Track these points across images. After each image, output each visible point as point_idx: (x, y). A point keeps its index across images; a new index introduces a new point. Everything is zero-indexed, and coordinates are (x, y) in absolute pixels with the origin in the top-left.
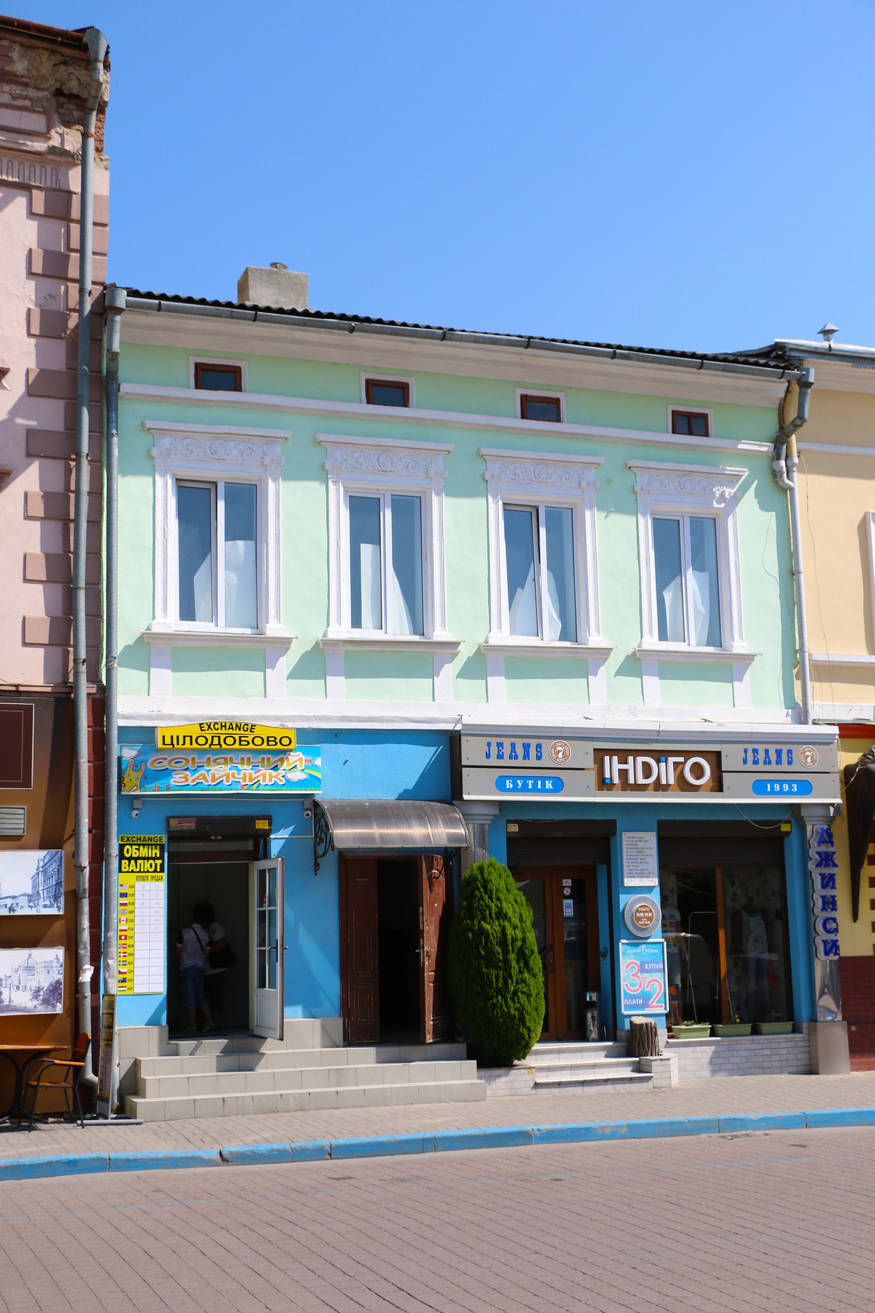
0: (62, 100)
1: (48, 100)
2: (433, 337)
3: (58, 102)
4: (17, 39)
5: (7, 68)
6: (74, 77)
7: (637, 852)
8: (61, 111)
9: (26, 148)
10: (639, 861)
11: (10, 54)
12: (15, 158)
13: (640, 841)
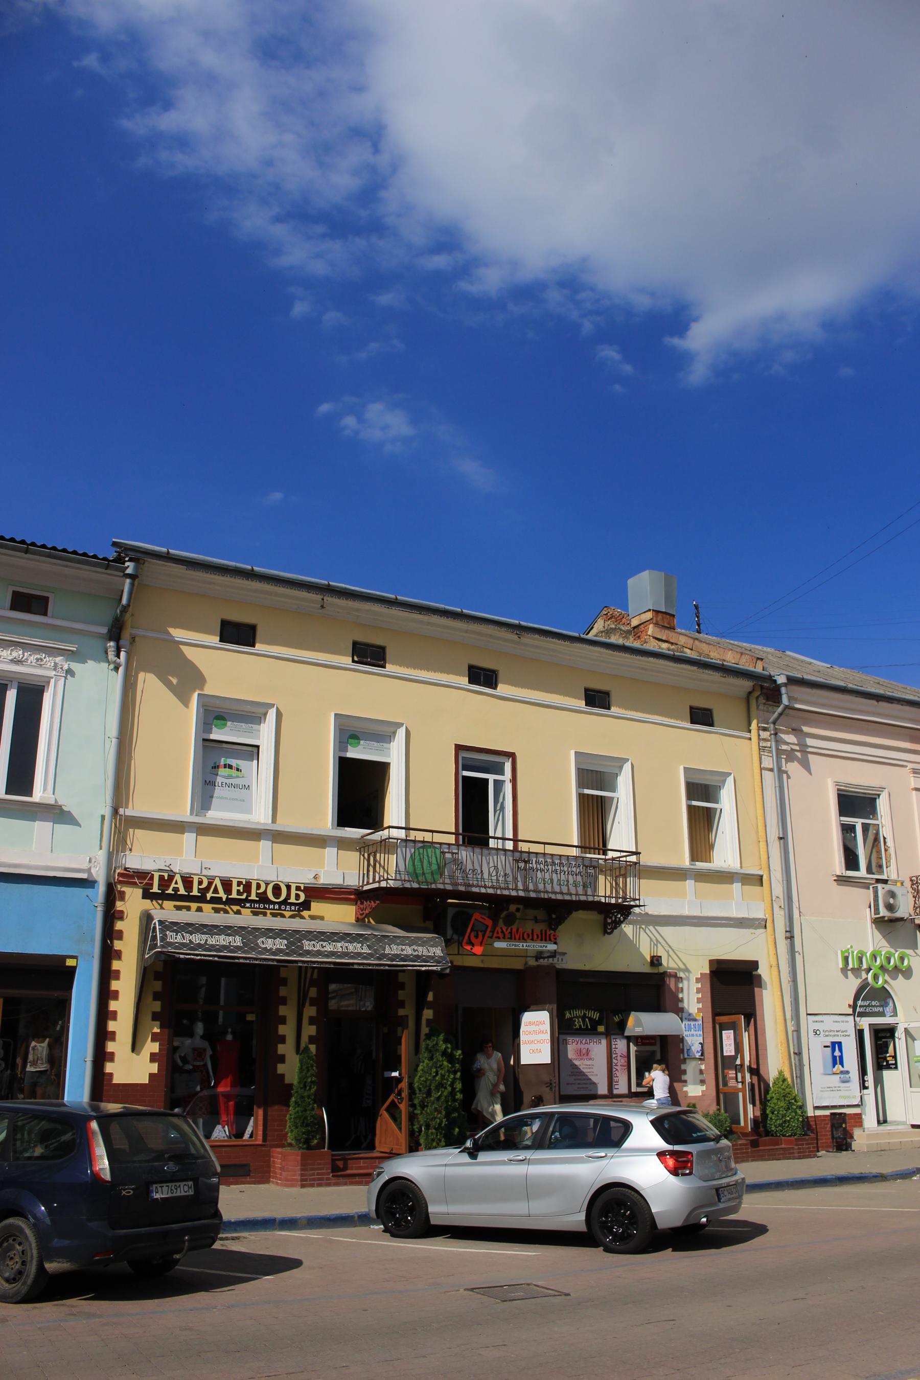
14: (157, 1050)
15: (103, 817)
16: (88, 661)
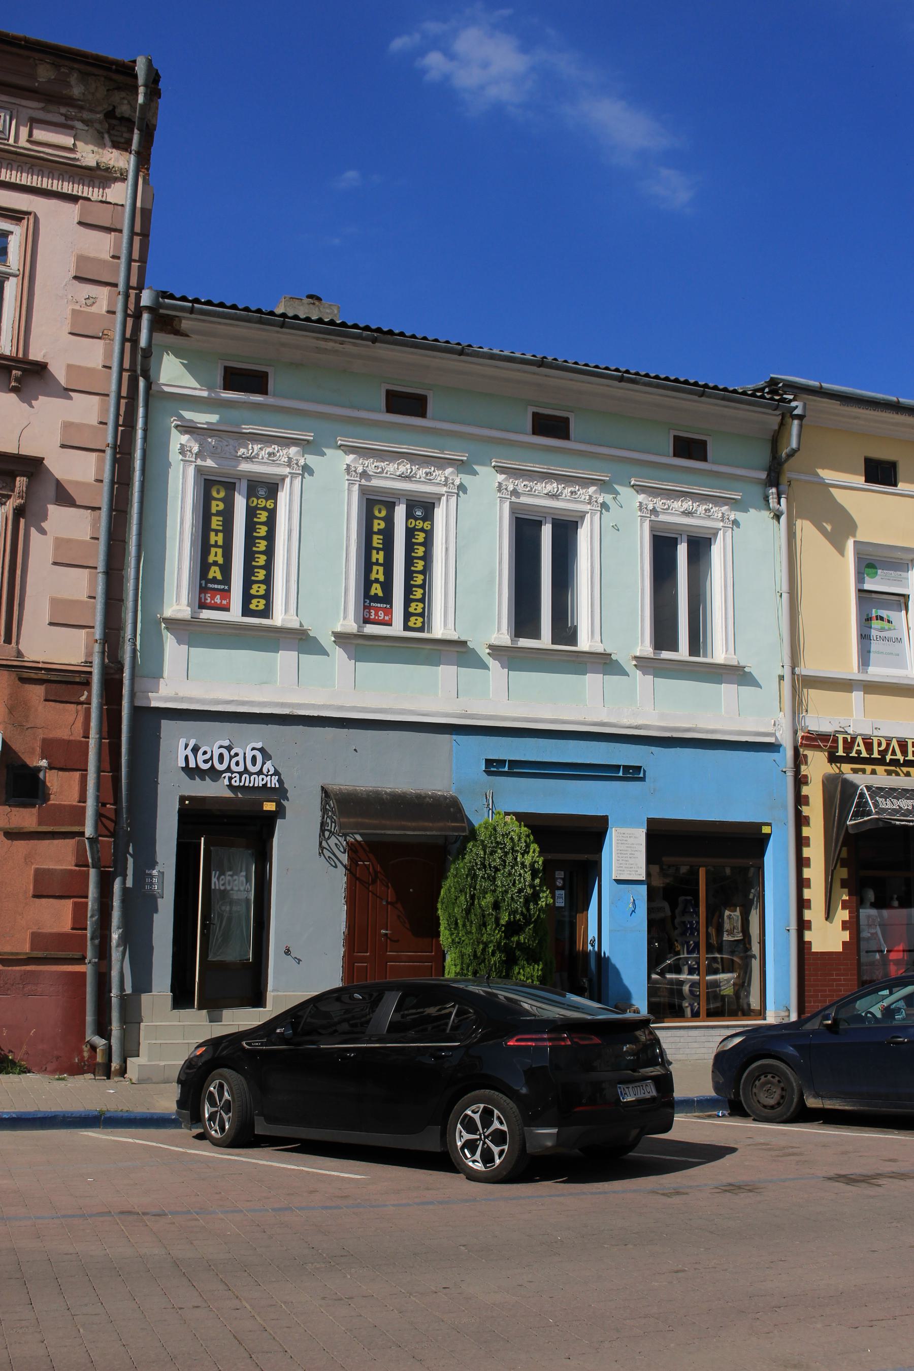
0: (114, 122)
1: (101, 122)
2: (451, 351)
3: (109, 124)
4: (76, 66)
5: (64, 92)
6: (126, 102)
7: (627, 847)
8: (111, 132)
9: (78, 163)
10: (629, 856)
11: (68, 80)
12: (66, 172)
13: (630, 837)
14: (847, 918)
15: (781, 678)
16: (750, 510)
